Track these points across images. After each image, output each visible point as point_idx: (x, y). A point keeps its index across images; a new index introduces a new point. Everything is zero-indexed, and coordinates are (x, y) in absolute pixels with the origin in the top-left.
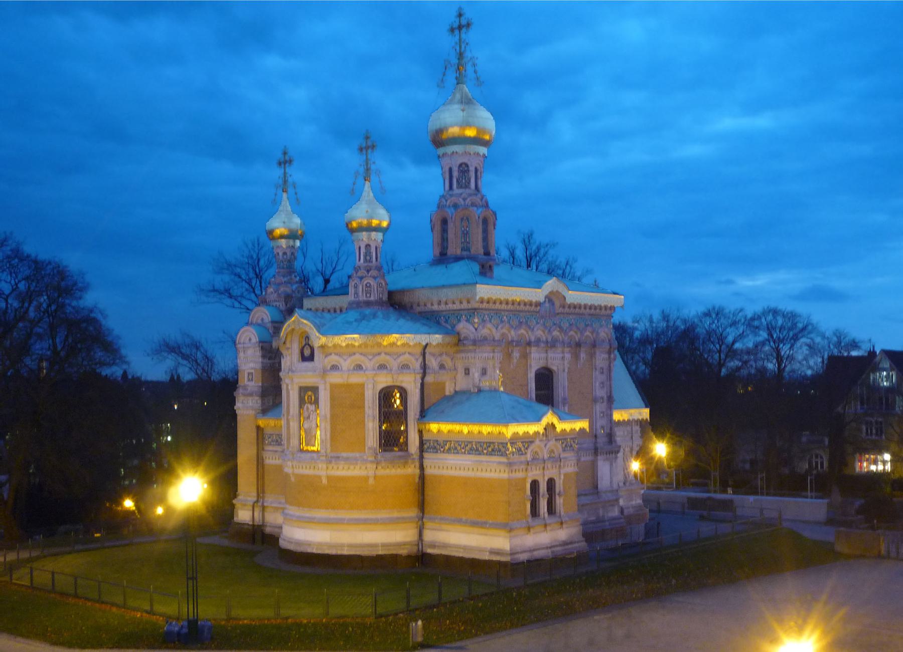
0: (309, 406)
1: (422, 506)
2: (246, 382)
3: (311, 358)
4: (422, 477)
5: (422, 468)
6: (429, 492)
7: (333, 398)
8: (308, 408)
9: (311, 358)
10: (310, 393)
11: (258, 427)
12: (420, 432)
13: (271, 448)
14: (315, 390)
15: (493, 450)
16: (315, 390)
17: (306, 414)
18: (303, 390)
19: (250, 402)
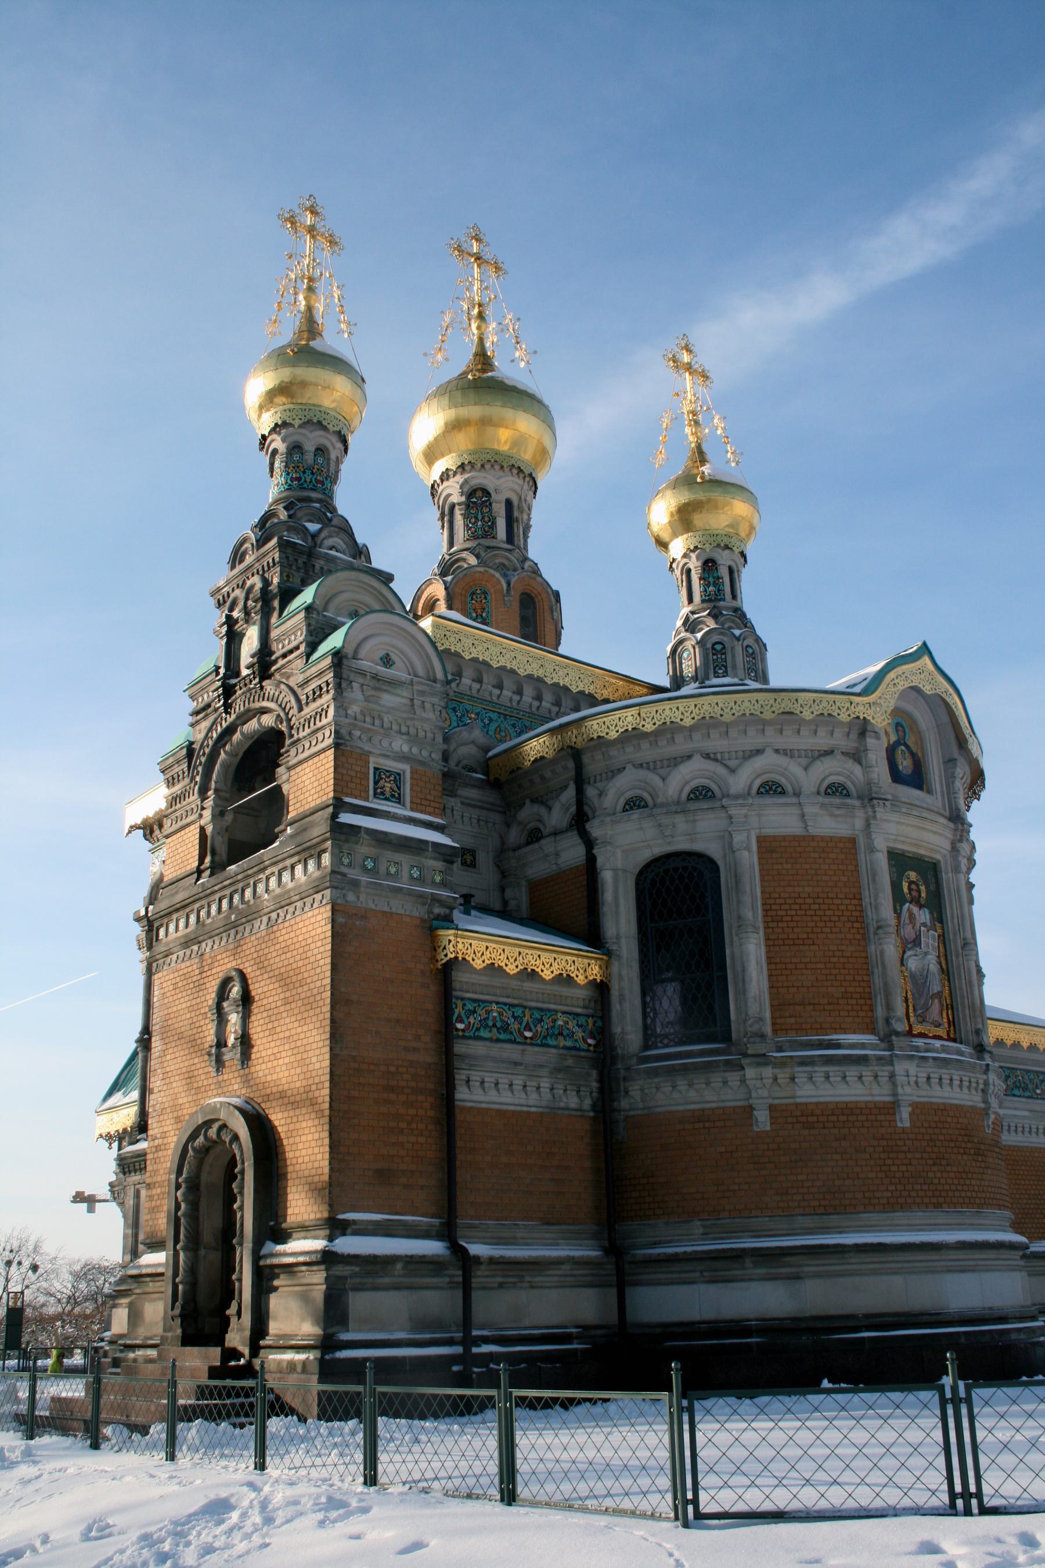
0: (915, 909)
8: (912, 916)
13: (477, 1048)
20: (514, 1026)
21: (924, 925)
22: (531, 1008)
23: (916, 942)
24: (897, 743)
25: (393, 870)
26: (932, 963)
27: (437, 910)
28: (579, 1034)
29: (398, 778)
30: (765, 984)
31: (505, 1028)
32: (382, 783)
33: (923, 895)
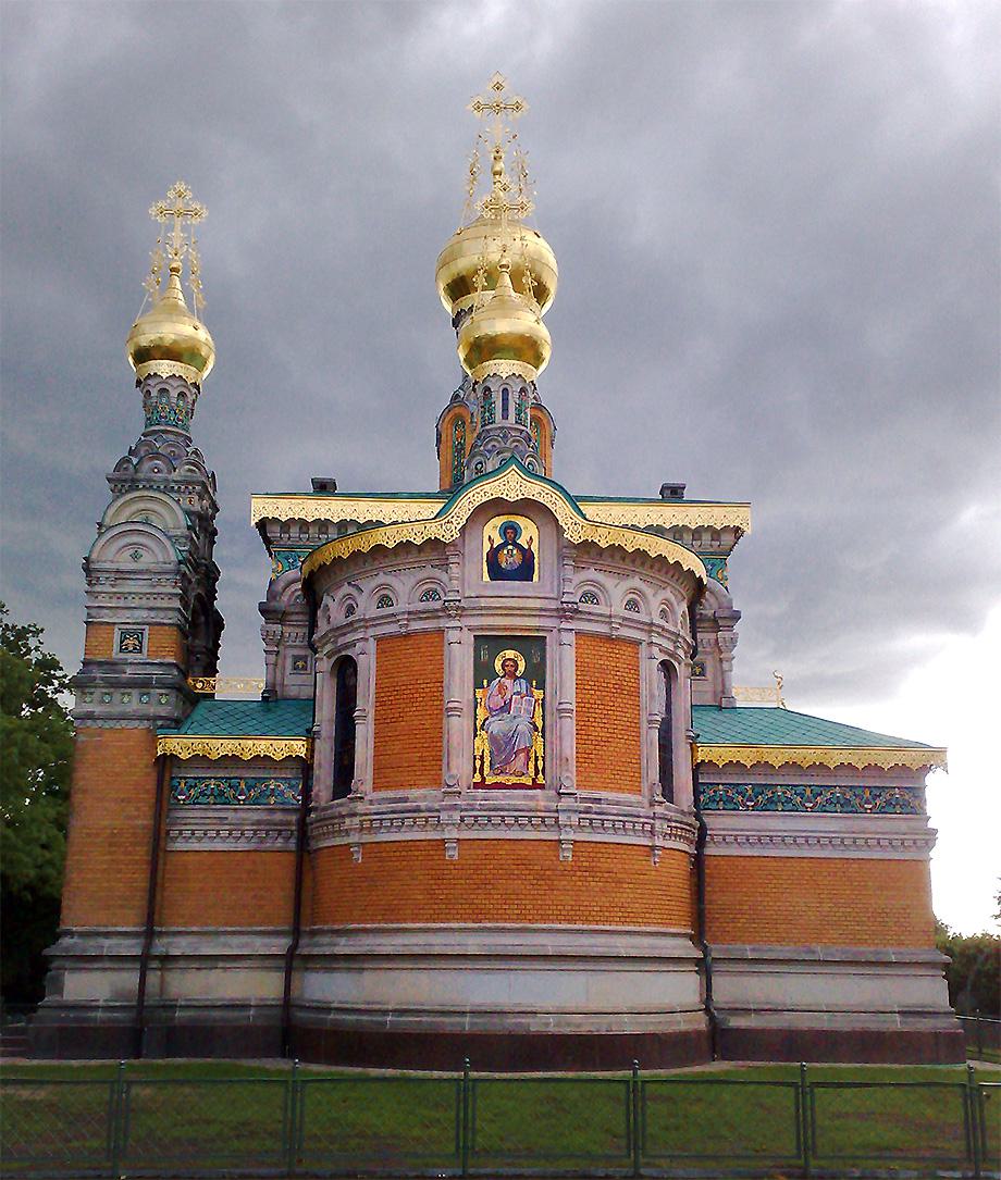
0: (508, 682)
1: (700, 926)
2: (116, 655)
3: (525, 571)
4: (698, 862)
5: (701, 843)
6: (716, 898)
7: (581, 667)
8: (502, 688)
9: (525, 571)
10: (510, 654)
11: (167, 762)
12: (697, 769)
14: (532, 645)
15: (888, 803)
16: (532, 645)
17: (498, 701)
18: (489, 643)
19: (135, 699)
20: (230, 793)
21: (518, 693)
22: (245, 778)
23: (506, 708)
24: (504, 545)
25: (126, 700)
26: (524, 727)
27: (160, 723)
28: (289, 794)
29: (139, 635)
30: (371, 752)
31: (222, 793)
32: (126, 642)
33: (522, 668)
